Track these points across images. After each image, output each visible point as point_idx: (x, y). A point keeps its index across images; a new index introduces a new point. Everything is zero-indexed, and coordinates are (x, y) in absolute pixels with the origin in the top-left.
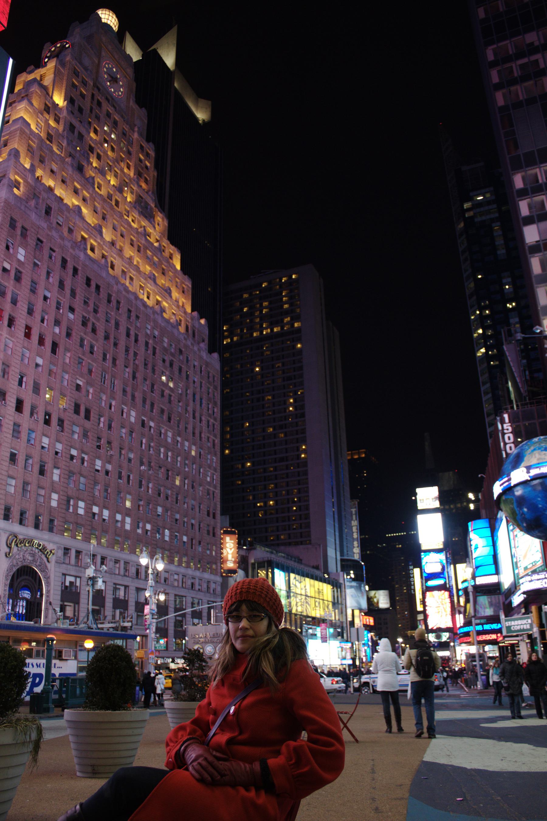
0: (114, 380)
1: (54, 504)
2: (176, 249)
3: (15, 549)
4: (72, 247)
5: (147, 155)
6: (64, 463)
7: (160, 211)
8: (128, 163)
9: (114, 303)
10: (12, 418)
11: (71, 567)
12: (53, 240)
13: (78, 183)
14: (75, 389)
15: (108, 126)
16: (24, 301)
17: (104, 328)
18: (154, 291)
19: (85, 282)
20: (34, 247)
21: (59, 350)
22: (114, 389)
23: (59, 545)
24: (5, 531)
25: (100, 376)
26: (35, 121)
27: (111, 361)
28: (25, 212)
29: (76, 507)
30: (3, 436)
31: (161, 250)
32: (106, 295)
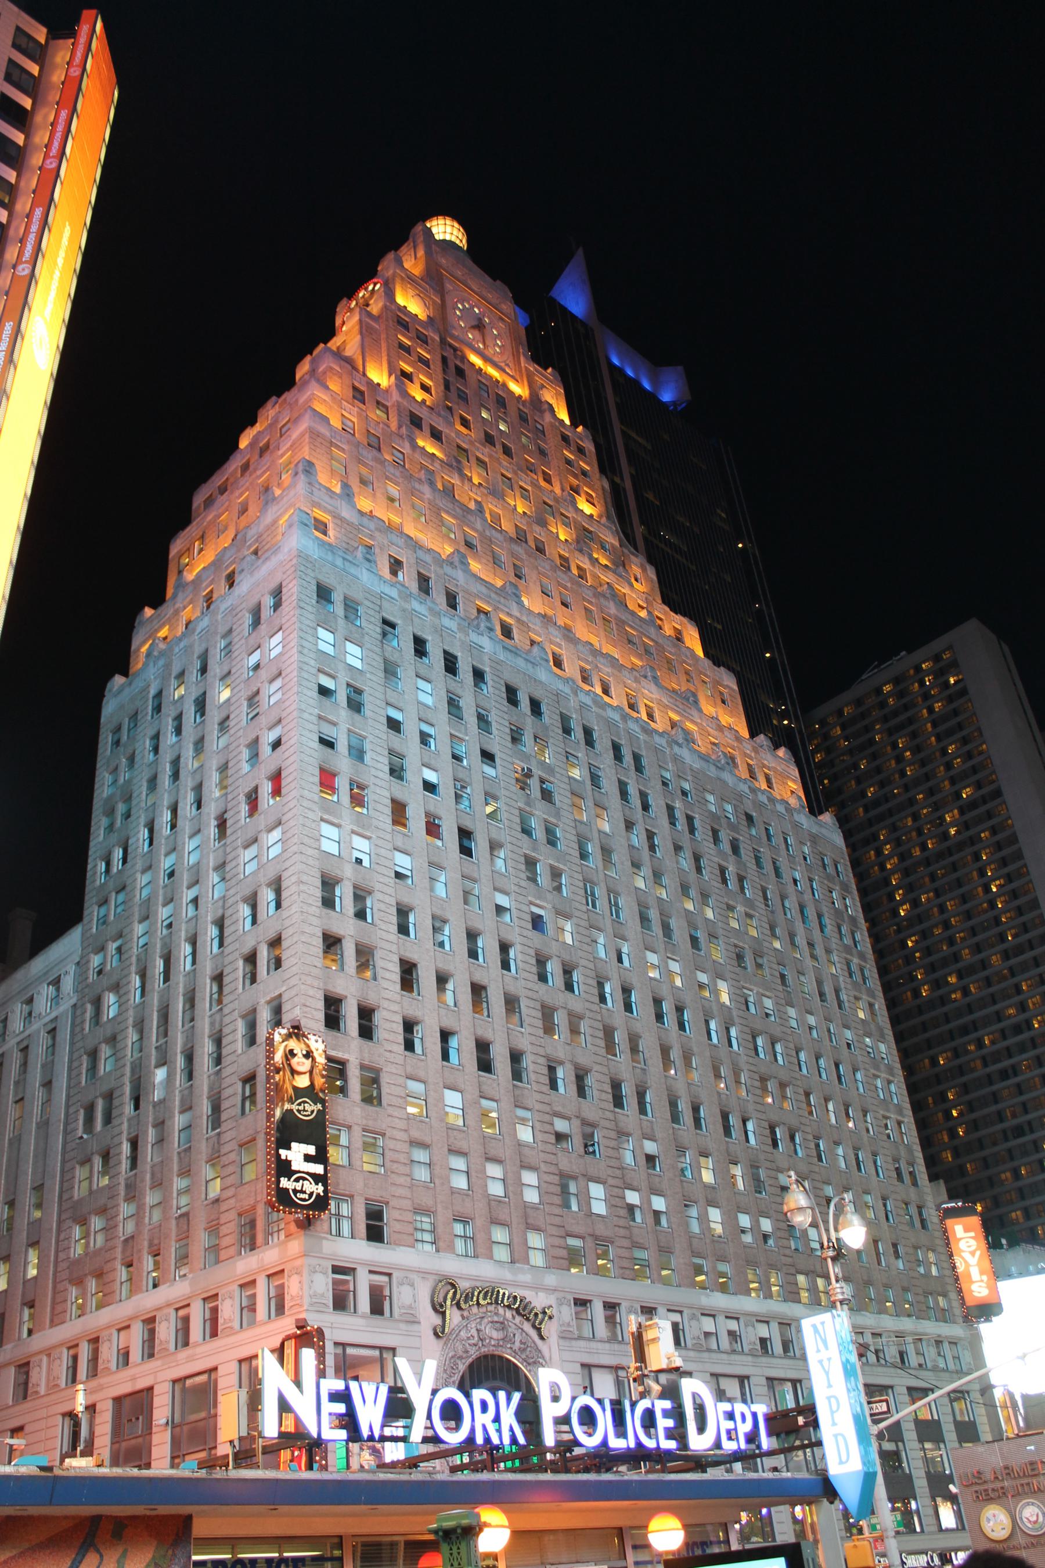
0: (616, 898)
1: (532, 1196)
2: (685, 620)
3: (454, 1316)
4: (460, 628)
5: (581, 451)
6: (538, 1097)
7: (633, 554)
8: (544, 472)
9: (578, 734)
10: (395, 1007)
11: (600, 1345)
12: (416, 620)
13: (447, 512)
14: (530, 926)
15: (488, 410)
16: (378, 749)
17: (568, 787)
18: (659, 702)
19: (504, 695)
20: (380, 637)
21: (476, 844)
22: (618, 916)
23: (561, 1295)
24: (424, 1273)
25: (582, 892)
26: (339, 416)
27: (599, 857)
28: (344, 570)
29: (585, 1199)
30: (382, 1051)
31: (653, 622)
32: (558, 718)
